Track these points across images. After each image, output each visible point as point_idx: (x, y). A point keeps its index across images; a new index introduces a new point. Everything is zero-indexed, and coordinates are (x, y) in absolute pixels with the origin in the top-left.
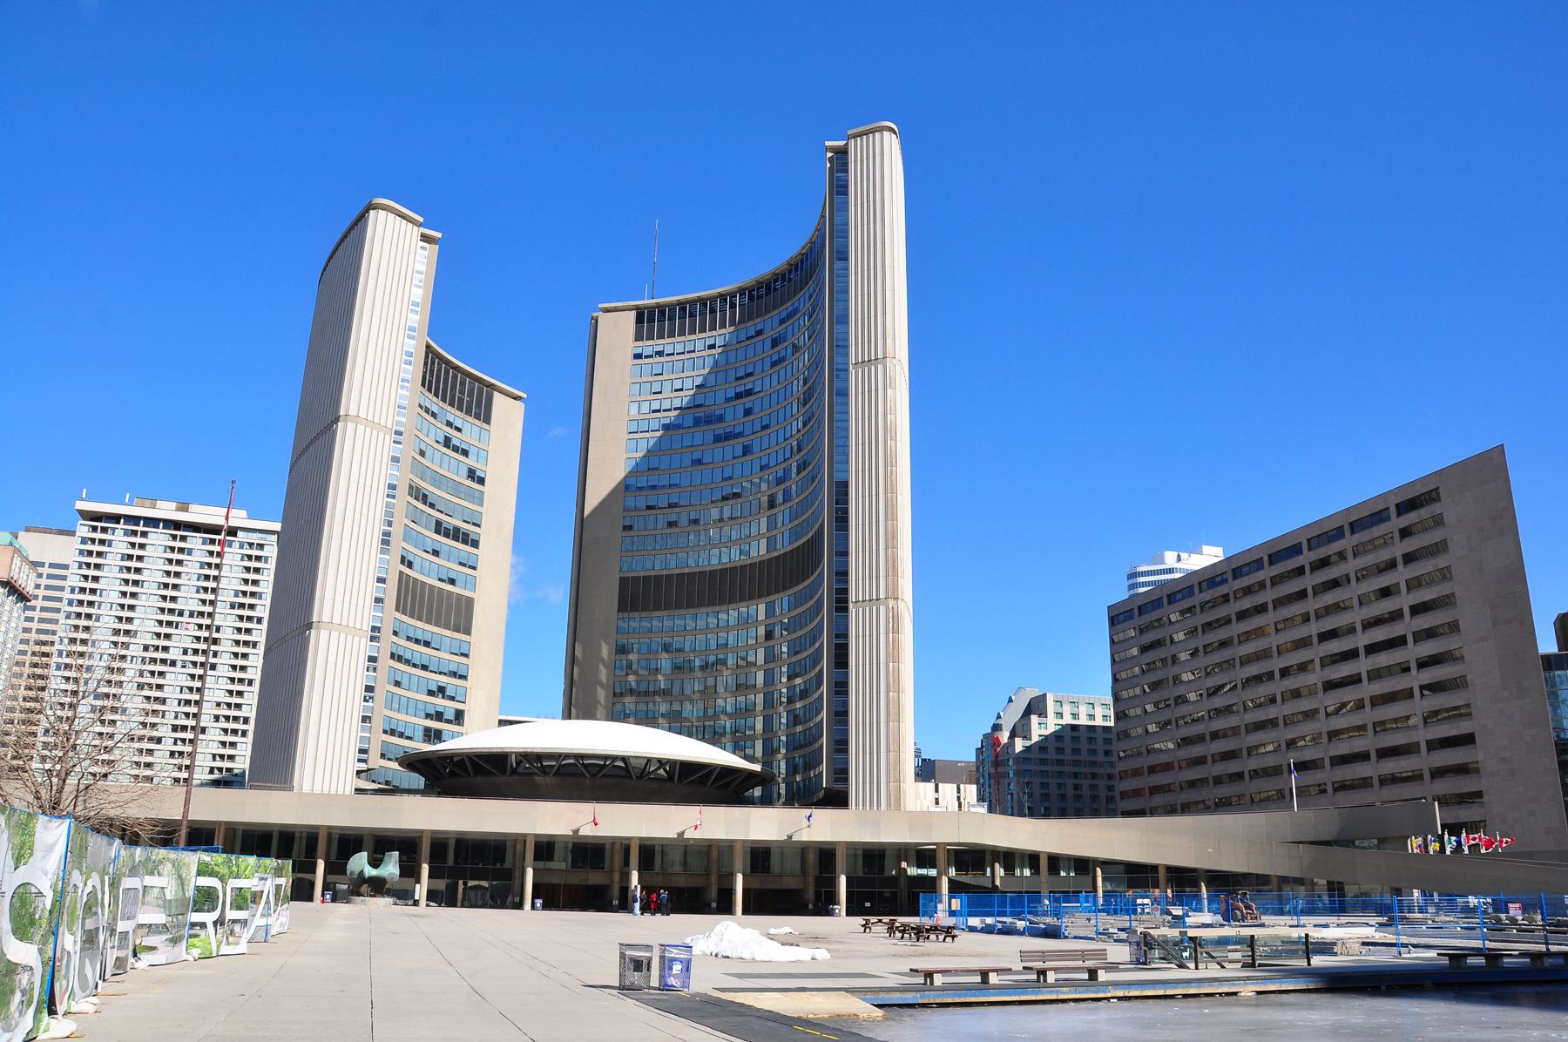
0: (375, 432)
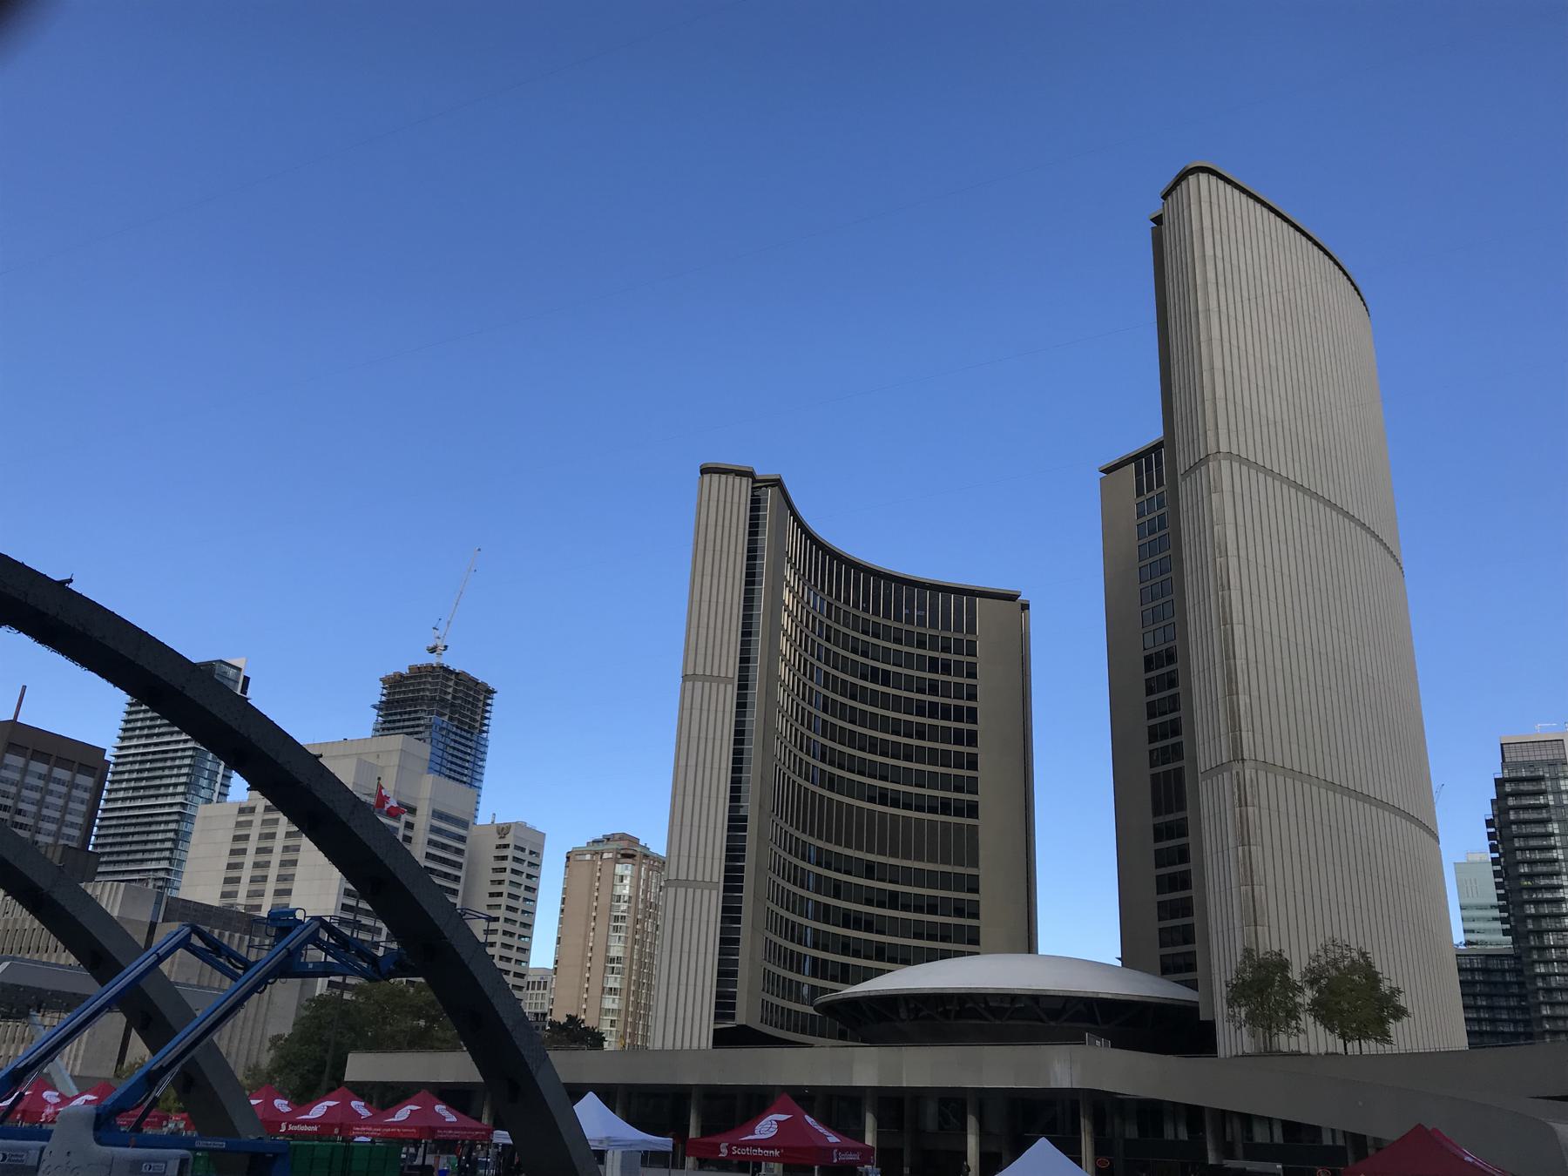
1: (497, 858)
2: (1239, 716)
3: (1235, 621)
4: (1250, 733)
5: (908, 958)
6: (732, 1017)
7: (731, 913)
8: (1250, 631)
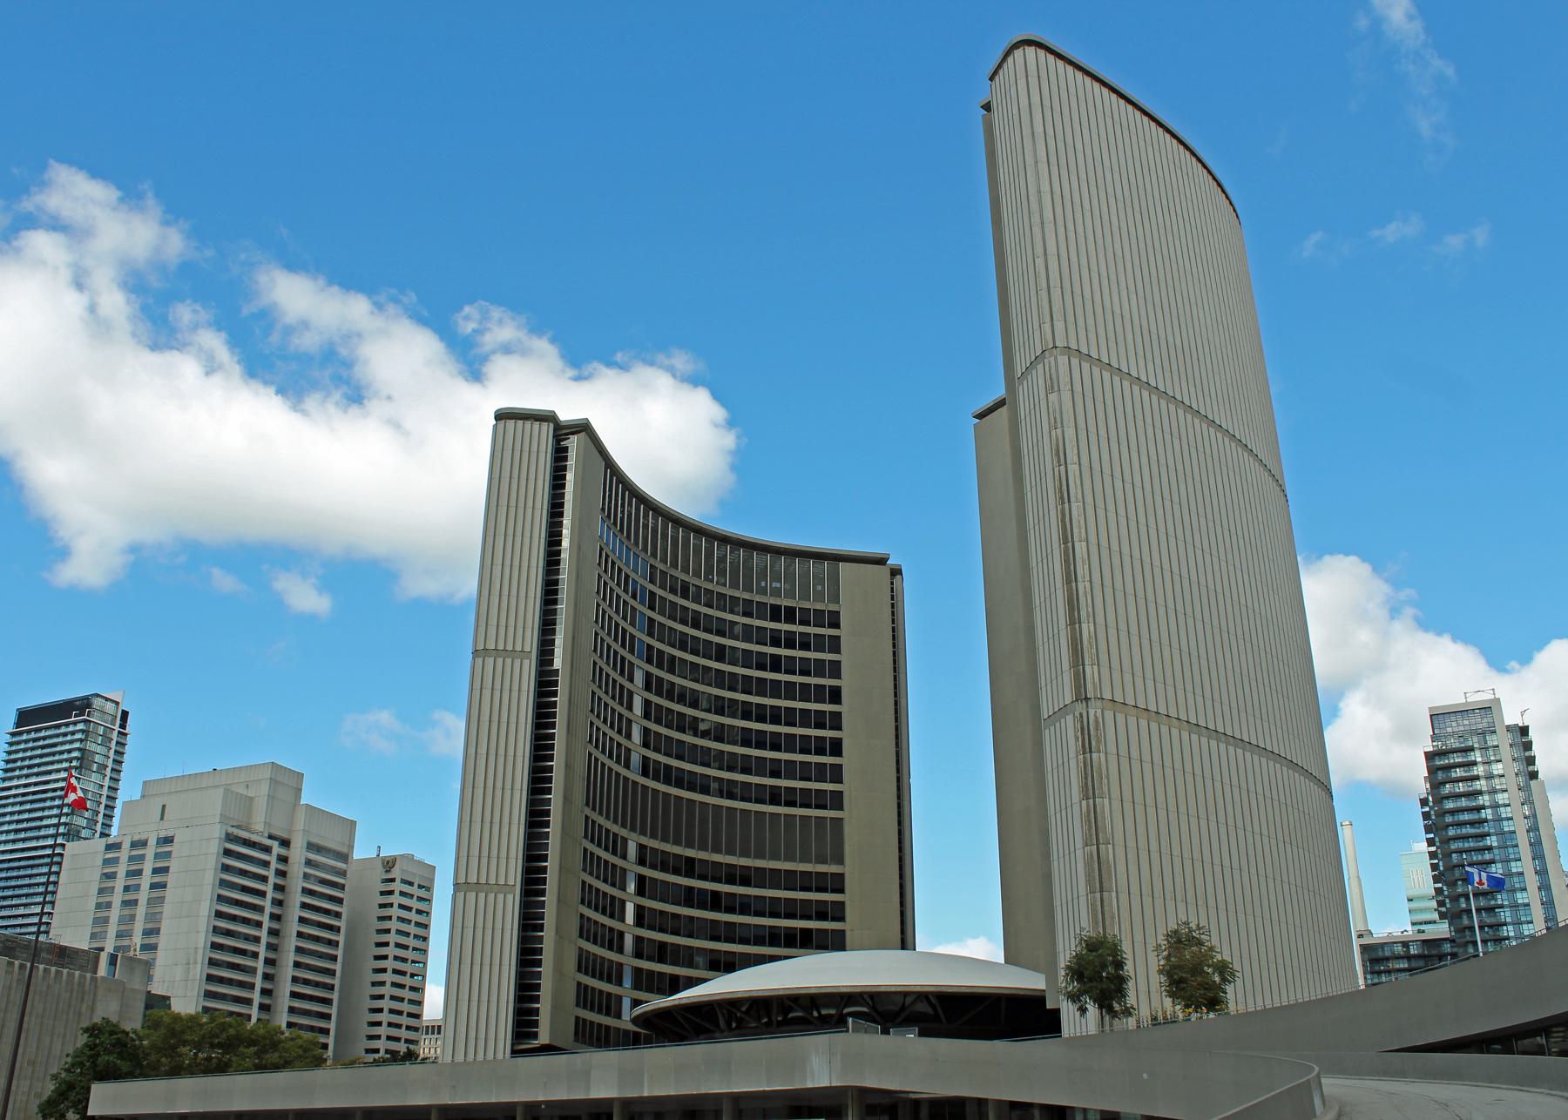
0: (509, 661)
1: (382, 893)
2: (1082, 648)
3: (1076, 539)
4: (1096, 667)
5: (728, 965)
6: (535, 1036)
7: (530, 922)
8: (1094, 549)
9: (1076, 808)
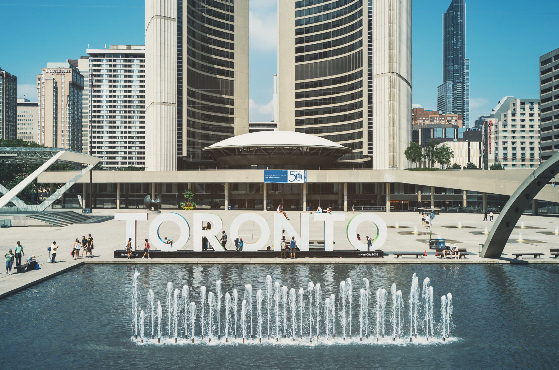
9: (387, 103)
